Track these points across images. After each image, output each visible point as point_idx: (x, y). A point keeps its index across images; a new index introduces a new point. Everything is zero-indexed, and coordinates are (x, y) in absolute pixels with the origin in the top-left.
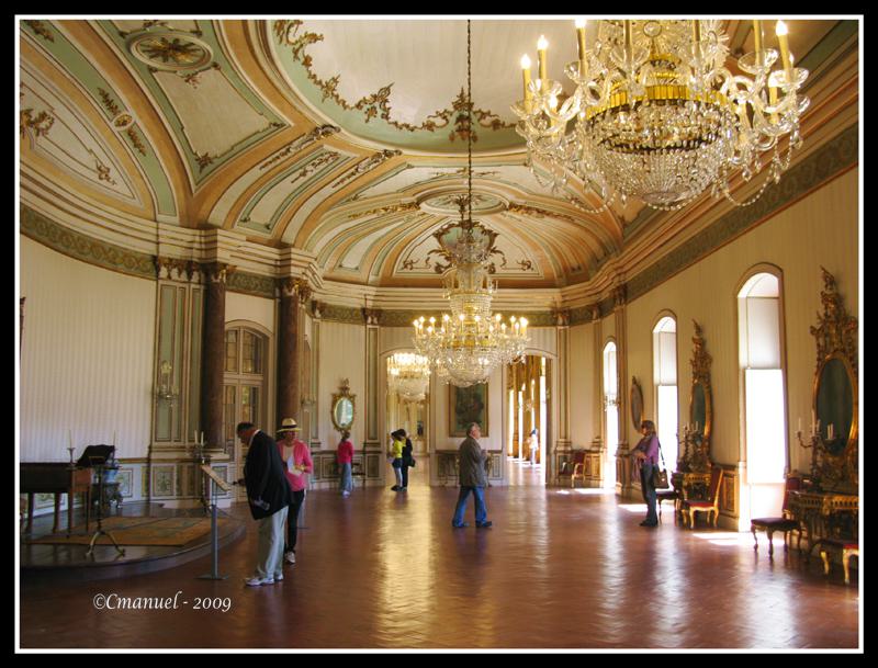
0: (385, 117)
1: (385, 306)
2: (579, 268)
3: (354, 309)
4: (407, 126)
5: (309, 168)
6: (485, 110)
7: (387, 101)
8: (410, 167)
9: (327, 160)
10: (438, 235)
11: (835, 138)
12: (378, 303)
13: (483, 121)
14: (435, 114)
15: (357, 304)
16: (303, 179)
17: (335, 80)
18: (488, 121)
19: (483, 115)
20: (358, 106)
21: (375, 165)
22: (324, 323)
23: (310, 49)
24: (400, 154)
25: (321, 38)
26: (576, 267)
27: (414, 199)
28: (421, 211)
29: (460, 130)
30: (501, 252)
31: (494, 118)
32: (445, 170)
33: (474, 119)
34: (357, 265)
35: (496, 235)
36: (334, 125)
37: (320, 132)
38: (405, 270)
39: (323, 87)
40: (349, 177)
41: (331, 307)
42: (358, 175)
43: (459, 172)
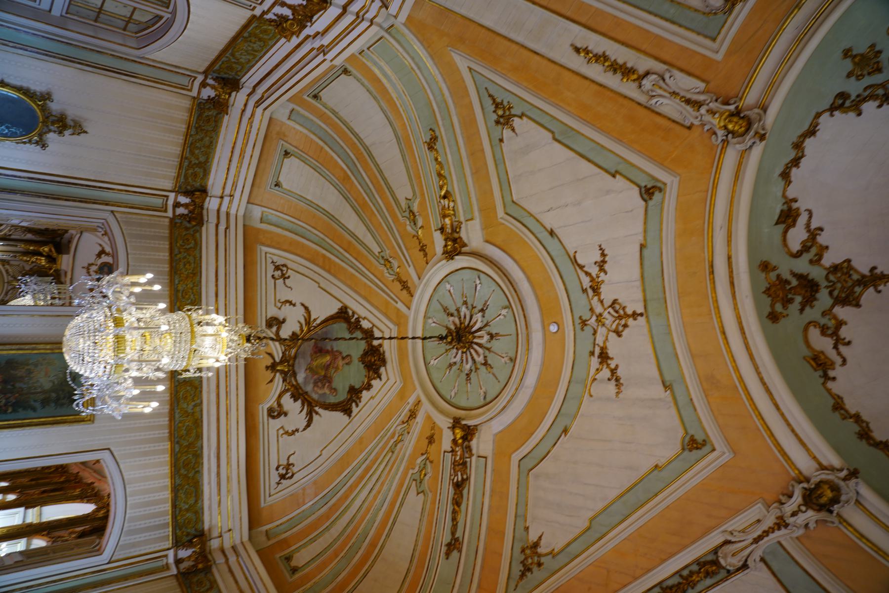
1: (208, 233)
2: (294, 570)
3: (206, 173)
6: (844, 332)
10: (343, 314)
12: (213, 219)
13: (814, 334)
15: (216, 181)
18: (823, 344)
19: (833, 331)
22: (186, 103)
26: (294, 563)
29: (782, 282)
30: (308, 425)
33: (812, 313)
34: (285, 185)
38: (271, 268)
41: (216, 129)
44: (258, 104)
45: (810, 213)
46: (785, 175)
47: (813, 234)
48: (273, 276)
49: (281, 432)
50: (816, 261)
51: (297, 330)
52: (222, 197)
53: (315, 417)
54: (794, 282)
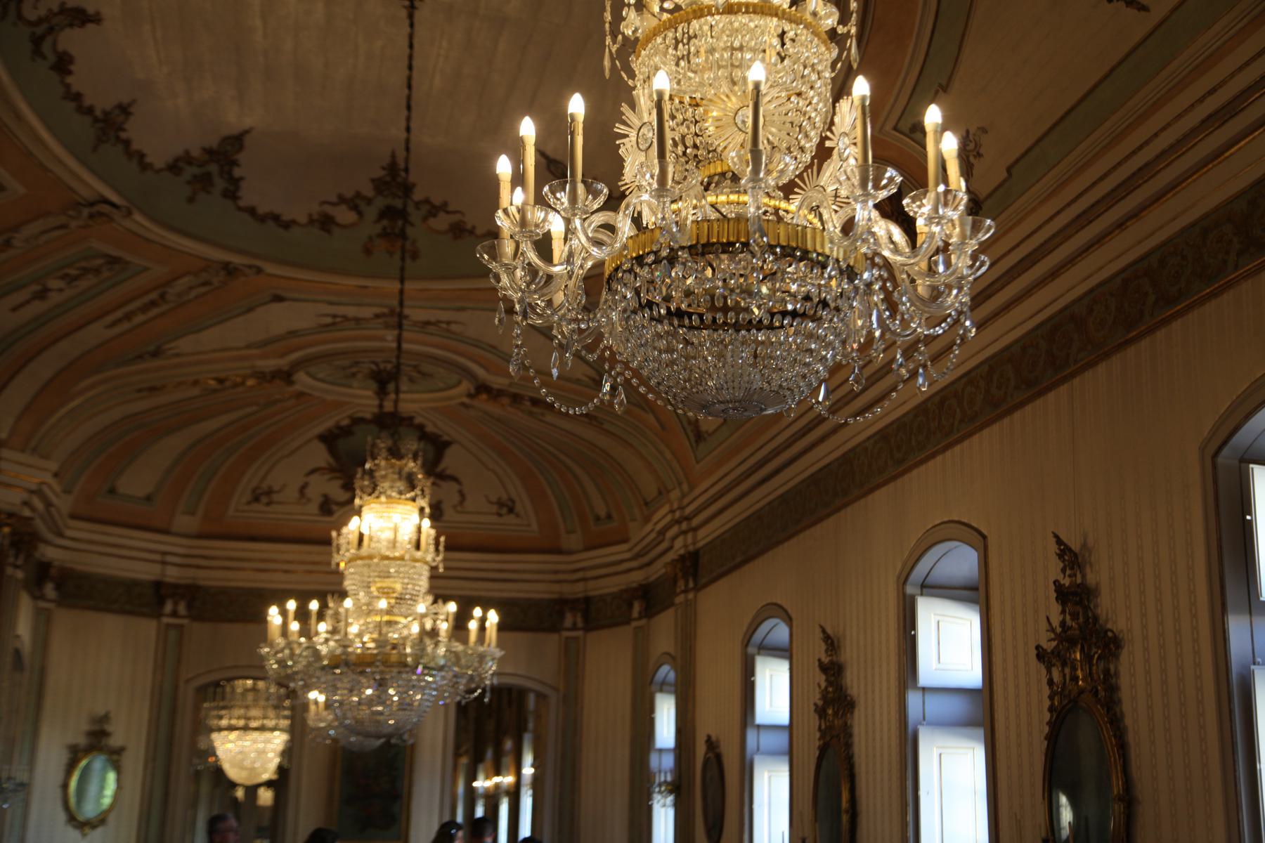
0: (231, 194)
1: (211, 578)
2: (609, 517)
3: (135, 583)
4: (276, 218)
5: (54, 284)
6: (437, 201)
7: (235, 163)
8: (278, 299)
9: (97, 271)
10: (330, 439)
11: (1080, 299)
12: (191, 573)
13: (432, 222)
14: (334, 199)
15: (145, 572)
16: (38, 307)
17: (125, 110)
18: (442, 222)
20: (174, 168)
21: (203, 290)
23: (71, 40)
24: (259, 271)
25: (96, 19)
27: (283, 363)
28: (298, 387)
29: (384, 235)
31: (456, 218)
32: (351, 311)
33: (415, 216)
35: (447, 444)
36: (115, 198)
37: (86, 212)
38: (256, 507)
39: (96, 120)
40: (144, 309)
42: (164, 308)
43: (377, 316)
44: (61, 535)
45: (324, 203)
46: (287, 225)
47: (342, 200)
48: (268, 504)
49: (459, 508)
50: (369, 201)
51: (340, 482)
52: (164, 563)
53: (448, 472)
54: (385, 222)
